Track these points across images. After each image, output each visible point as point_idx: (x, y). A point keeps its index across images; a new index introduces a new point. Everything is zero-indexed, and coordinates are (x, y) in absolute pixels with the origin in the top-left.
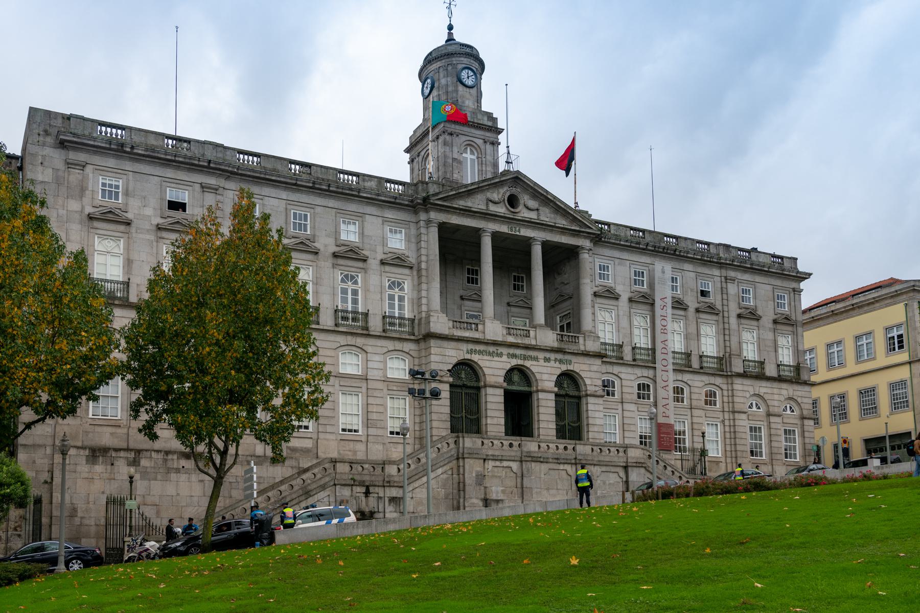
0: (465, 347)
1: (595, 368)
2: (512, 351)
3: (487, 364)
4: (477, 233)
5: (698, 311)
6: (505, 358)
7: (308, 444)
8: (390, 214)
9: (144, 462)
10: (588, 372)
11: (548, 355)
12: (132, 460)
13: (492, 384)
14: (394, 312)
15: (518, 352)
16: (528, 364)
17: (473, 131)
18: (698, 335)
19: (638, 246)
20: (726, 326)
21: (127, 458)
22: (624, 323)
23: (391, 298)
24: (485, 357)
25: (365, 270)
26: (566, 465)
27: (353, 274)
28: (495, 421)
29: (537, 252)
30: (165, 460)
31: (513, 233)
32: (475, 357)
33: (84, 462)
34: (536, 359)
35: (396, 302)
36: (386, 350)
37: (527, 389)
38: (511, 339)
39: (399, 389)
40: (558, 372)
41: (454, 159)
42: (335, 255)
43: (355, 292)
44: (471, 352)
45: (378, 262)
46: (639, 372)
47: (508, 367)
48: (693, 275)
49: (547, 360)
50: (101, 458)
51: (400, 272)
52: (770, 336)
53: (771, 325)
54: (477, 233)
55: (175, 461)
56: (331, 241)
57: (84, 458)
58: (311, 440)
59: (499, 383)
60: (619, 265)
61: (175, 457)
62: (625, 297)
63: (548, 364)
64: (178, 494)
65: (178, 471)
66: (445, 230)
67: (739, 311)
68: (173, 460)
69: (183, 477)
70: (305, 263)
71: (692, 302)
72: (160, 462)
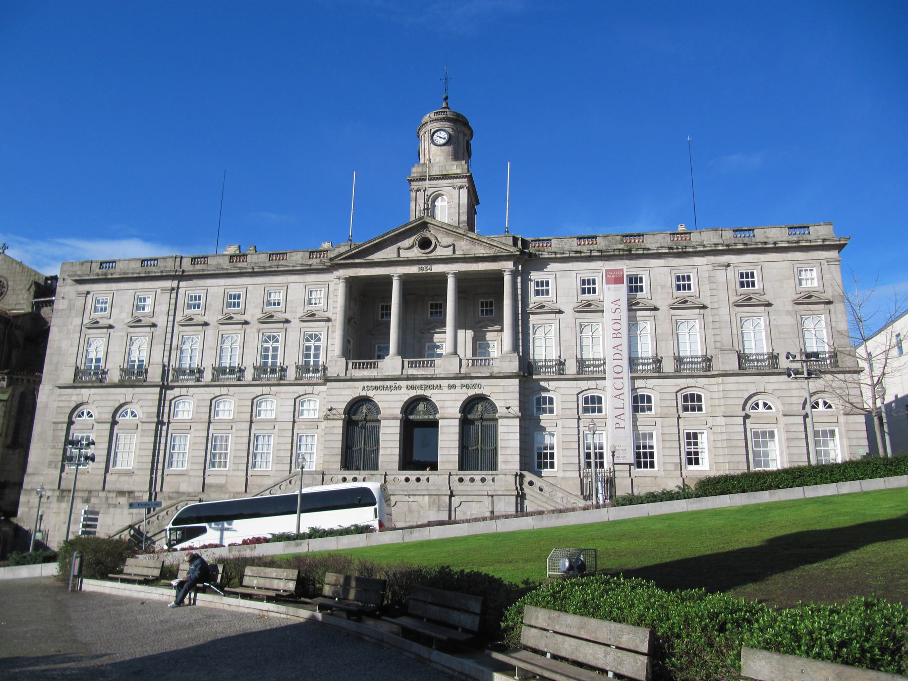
1: (511, 389)
2: (411, 383)
3: (384, 398)
4: (388, 280)
6: (404, 390)
7: (221, 480)
9: (93, 500)
10: (501, 394)
11: (452, 382)
12: (85, 498)
13: (386, 416)
14: (319, 361)
16: (428, 393)
17: (441, 182)
19: (579, 255)
20: (717, 318)
21: (82, 497)
23: (308, 348)
24: (383, 392)
26: (417, 497)
27: (274, 334)
28: (388, 452)
30: (107, 498)
31: (424, 272)
32: (370, 394)
33: (56, 501)
35: (312, 352)
36: (297, 395)
37: (431, 417)
39: (307, 427)
40: (464, 397)
44: (368, 388)
45: (298, 320)
47: (406, 398)
49: (451, 387)
50: (66, 498)
51: (316, 326)
53: (790, 307)
55: (114, 499)
56: (259, 310)
57: (56, 498)
58: (225, 477)
59: (393, 415)
60: (561, 277)
61: (114, 495)
62: (568, 309)
63: (453, 390)
64: (113, 524)
65: (115, 506)
66: (352, 284)
67: (734, 299)
68: (112, 497)
69: (118, 511)
70: (234, 332)
71: (663, 300)
72: (104, 499)
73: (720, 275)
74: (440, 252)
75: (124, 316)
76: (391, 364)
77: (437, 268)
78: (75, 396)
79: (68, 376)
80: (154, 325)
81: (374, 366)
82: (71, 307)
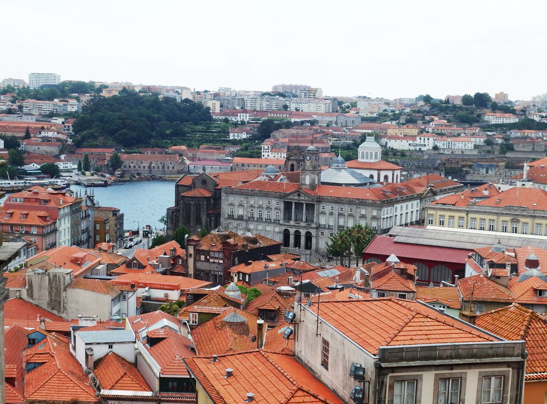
5: (348, 216)
8: (276, 199)
16: (299, 230)
18: (348, 221)
22: (327, 219)
29: (304, 205)
32: (288, 229)
38: (296, 225)
41: (304, 179)
42: (266, 208)
46: (330, 231)
52: (370, 222)
67: (360, 216)
71: (346, 214)
74: (302, 198)
76: (292, 223)
77: (301, 202)
78: (228, 221)
79: (226, 216)
81: (289, 222)
82: (225, 199)
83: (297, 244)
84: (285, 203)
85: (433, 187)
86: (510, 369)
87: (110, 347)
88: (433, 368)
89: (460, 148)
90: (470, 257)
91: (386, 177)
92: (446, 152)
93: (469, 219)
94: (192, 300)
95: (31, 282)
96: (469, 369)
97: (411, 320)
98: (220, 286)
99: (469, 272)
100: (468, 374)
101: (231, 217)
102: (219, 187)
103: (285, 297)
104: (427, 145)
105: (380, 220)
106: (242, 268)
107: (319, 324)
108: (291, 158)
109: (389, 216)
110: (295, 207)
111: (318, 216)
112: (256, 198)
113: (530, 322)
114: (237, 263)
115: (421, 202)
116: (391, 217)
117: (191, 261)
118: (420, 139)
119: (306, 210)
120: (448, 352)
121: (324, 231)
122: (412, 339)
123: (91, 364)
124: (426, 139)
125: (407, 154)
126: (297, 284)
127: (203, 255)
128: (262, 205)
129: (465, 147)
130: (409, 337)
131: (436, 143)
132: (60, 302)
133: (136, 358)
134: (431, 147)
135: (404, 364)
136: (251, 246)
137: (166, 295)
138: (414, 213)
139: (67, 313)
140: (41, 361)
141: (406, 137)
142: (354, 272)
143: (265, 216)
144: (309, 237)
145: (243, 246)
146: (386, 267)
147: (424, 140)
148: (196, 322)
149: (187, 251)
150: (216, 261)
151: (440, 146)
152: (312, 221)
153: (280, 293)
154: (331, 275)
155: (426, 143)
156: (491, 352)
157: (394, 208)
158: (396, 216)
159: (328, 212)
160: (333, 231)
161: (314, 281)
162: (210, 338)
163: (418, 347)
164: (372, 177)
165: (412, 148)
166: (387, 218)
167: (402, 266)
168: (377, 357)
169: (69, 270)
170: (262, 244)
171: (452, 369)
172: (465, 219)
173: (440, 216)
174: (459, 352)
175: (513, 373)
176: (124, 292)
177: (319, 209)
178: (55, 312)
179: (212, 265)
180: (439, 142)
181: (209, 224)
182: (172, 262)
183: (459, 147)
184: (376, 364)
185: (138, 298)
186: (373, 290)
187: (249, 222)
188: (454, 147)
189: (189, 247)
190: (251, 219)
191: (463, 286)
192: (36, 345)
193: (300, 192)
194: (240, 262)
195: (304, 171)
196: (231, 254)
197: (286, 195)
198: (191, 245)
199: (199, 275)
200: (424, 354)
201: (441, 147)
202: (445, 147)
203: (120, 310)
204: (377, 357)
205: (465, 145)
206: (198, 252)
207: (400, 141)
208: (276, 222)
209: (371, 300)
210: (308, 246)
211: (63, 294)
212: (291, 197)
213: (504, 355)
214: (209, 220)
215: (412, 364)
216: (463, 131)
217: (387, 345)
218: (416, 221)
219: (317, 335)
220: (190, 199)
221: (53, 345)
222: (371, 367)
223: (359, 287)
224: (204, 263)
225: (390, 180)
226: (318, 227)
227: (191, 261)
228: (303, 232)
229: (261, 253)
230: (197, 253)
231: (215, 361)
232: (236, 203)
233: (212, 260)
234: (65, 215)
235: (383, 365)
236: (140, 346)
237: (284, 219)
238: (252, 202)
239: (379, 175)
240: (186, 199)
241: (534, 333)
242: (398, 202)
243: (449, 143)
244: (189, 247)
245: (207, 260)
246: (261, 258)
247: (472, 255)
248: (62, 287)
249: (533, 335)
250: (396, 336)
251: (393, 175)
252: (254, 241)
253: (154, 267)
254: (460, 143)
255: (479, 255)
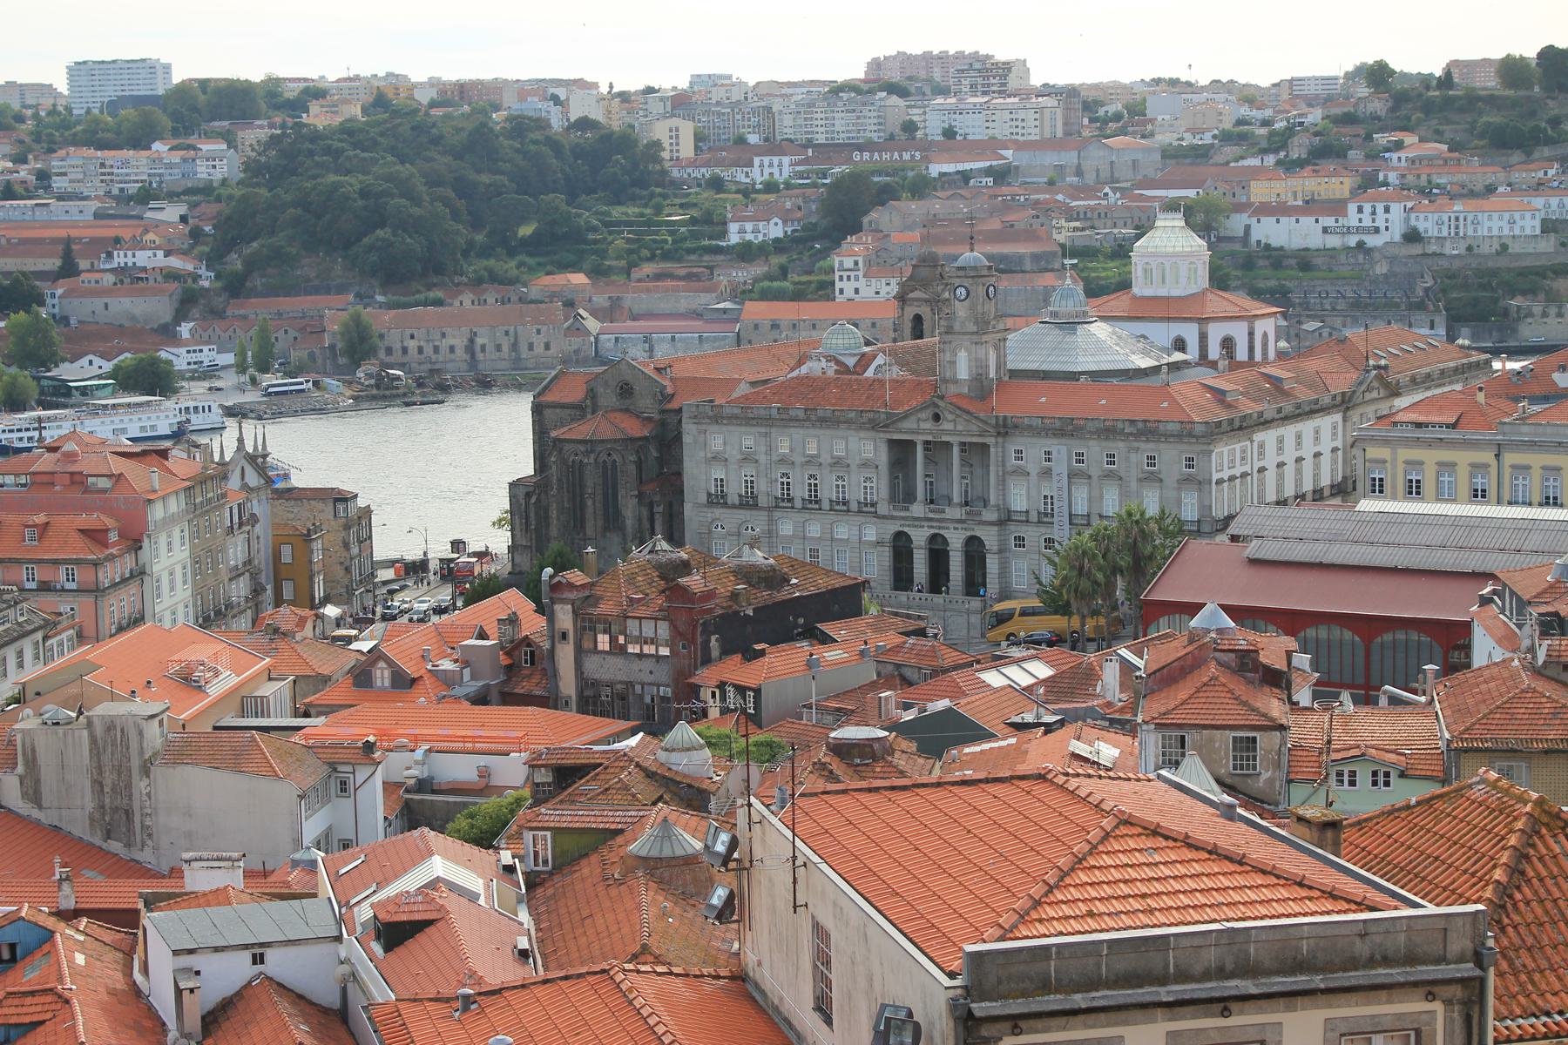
0: (899, 522)
8: (862, 434)
15: (934, 524)
16: (942, 532)
18: (1102, 497)
25: (849, 472)
29: (956, 450)
32: (906, 529)
34: (948, 528)
38: (931, 515)
43: (843, 486)
44: (903, 525)
46: (1042, 529)
48: (1098, 449)
49: (956, 529)
52: (1173, 494)
53: (1176, 485)
54: (910, 445)
62: (1034, 473)
73: (1133, 456)
74: (949, 426)
75: (735, 452)
76: (918, 509)
77: (945, 438)
79: (703, 498)
80: (757, 461)
81: (907, 509)
83: (938, 580)
84: (892, 443)
85: (1385, 368)
86: (1437, 1007)
87: (258, 959)
88: (1159, 1012)
89: (1495, 232)
90: (1485, 601)
91: (1228, 344)
92: (1448, 250)
93: (1507, 471)
94: (549, 786)
95: (33, 751)
96: (1289, 1009)
97: (1095, 847)
98: (641, 734)
99: (1484, 649)
100: (1285, 1029)
101: (717, 500)
102: (674, 405)
103: (858, 761)
104: (1383, 228)
105: (1207, 486)
106: (734, 670)
107: (801, 872)
108: (911, 295)
109: (1237, 472)
110: (926, 457)
111: (1002, 482)
112: (797, 433)
113: (1532, 833)
114: (715, 653)
115: (1345, 420)
116: (1244, 475)
117: (566, 655)
118: (1360, 210)
119: (962, 466)
120: (1211, 957)
121: (1022, 531)
122: (1091, 914)
123: (193, 1023)
124: (1380, 208)
125: (1318, 261)
126: (909, 716)
127: (605, 632)
128: (818, 456)
129: (1511, 229)
130: (1084, 908)
131: (1413, 222)
132: (129, 814)
133: (344, 991)
134: (1396, 234)
135: (1053, 1002)
136: (764, 596)
137: (484, 773)
138: (1326, 460)
139: (156, 849)
140: (27, 1020)
141: (1312, 206)
142: (1101, 668)
143: (827, 493)
144: (975, 553)
145: (734, 596)
146: (1190, 648)
147: (1374, 213)
148: (545, 862)
149: (551, 620)
150: (649, 649)
151: (1426, 231)
152: (986, 503)
153: (843, 750)
154: (1026, 680)
155: (1380, 223)
156: (1362, 949)
157: (1255, 445)
158: (1262, 470)
159: (1033, 469)
160: (1056, 530)
161: (963, 701)
162: (585, 913)
163: (1102, 942)
164: (1180, 345)
165: (1333, 241)
166: (1232, 478)
167: (1244, 638)
168: (958, 982)
169: (155, 708)
170: (797, 586)
171: (1226, 1013)
172: (1493, 471)
173: (1407, 462)
174: (1247, 953)
175: (1448, 1021)
176: (341, 768)
177: (1003, 461)
178: (115, 846)
179: (637, 665)
180: (1422, 216)
181: (646, 525)
182: (504, 660)
183: (1490, 229)
184: (954, 1005)
185: (390, 787)
186: (1145, 727)
187: (777, 514)
188: (1475, 230)
189: (557, 607)
190: (784, 501)
191: (1452, 700)
192: (20, 965)
193: (938, 406)
194: (726, 651)
195: (950, 337)
196: (695, 627)
197: (891, 421)
198: (563, 601)
199: (593, 700)
200: (1122, 964)
201: (1430, 234)
202: (1445, 233)
203: (330, 828)
204: (958, 982)
205: (1512, 222)
206: (587, 624)
207: (1294, 219)
208: (867, 509)
209: (980, 781)
210: (974, 584)
211: (140, 785)
212: (910, 424)
213: (1411, 959)
214: (645, 512)
215: (1079, 1000)
216: (1501, 176)
217: (1002, 939)
218: (1332, 486)
219: (795, 907)
220: (582, 448)
221: (71, 961)
222: (940, 1018)
223: (1117, 716)
224: (611, 660)
225: (1241, 354)
226: (1006, 518)
227: (566, 655)
228: (956, 540)
229: (796, 618)
230: (584, 628)
231: (466, 1009)
232: (733, 454)
233: (633, 649)
234: (169, 521)
235: (980, 1008)
236: (352, 948)
237: (893, 499)
238: (784, 449)
239: (1203, 338)
240: (567, 447)
241: (1544, 873)
242: (1265, 423)
243: (1457, 219)
244: (557, 607)
245: (618, 650)
246: (799, 634)
247: (1494, 592)
248: (135, 763)
249: (1541, 880)
250: (1037, 903)
251: (1251, 334)
252: (772, 579)
253: (447, 680)
254: (1495, 216)
255: (1512, 593)
